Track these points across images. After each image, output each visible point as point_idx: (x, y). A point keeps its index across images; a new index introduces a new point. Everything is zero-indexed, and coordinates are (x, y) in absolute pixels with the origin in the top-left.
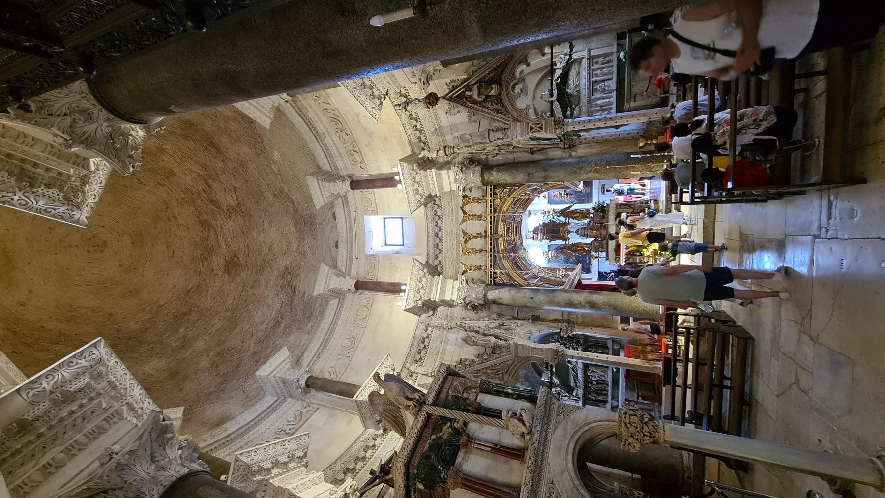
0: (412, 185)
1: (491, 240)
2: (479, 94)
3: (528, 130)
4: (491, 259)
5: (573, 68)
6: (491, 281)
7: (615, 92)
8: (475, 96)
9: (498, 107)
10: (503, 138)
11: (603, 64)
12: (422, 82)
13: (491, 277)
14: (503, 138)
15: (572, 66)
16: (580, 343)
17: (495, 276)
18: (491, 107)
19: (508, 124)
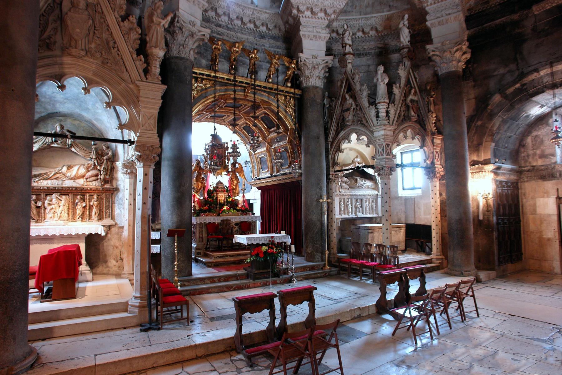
0: (318, 5)
1: (246, 83)
2: (412, 101)
3: (387, 141)
4: (223, 78)
5: (372, 184)
6: (196, 73)
7: (356, 216)
8: (411, 97)
9: (402, 117)
10: (377, 116)
11: (372, 206)
12: (434, 49)
13: (201, 74)
14: (377, 116)
15: (373, 182)
16: (104, 185)
17: (199, 80)
18: (402, 110)
19: (393, 124)
